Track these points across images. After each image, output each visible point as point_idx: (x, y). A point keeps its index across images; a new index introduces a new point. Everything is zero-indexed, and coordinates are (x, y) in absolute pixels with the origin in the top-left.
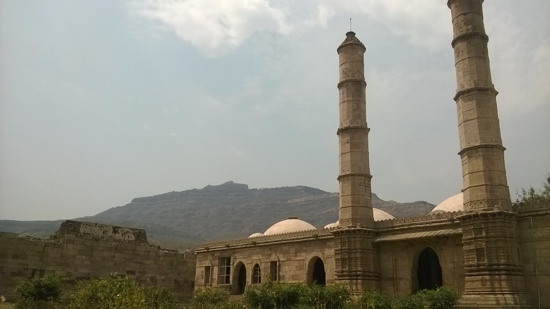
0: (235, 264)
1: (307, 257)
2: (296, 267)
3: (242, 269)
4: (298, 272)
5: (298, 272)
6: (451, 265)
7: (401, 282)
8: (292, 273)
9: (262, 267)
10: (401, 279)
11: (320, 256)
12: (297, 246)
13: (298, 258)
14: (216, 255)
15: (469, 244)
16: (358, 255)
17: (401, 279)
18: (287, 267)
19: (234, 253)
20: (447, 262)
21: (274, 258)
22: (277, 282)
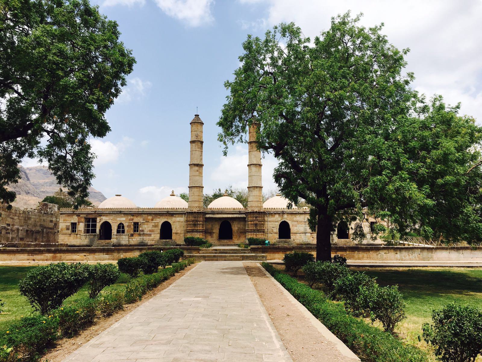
0: (102, 222)
1: (161, 221)
2: (153, 226)
3: (106, 226)
4: (153, 229)
5: (153, 229)
6: (237, 228)
7: (214, 234)
8: (150, 229)
9: (126, 225)
10: (214, 233)
11: (169, 221)
12: (153, 215)
13: (153, 221)
14: (81, 216)
15: (251, 222)
16: (201, 223)
17: (214, 233)
18: (146, 226)
19: (101, 216)
20: (235, 227)
21: (136, 220)
22: (138, 233)
